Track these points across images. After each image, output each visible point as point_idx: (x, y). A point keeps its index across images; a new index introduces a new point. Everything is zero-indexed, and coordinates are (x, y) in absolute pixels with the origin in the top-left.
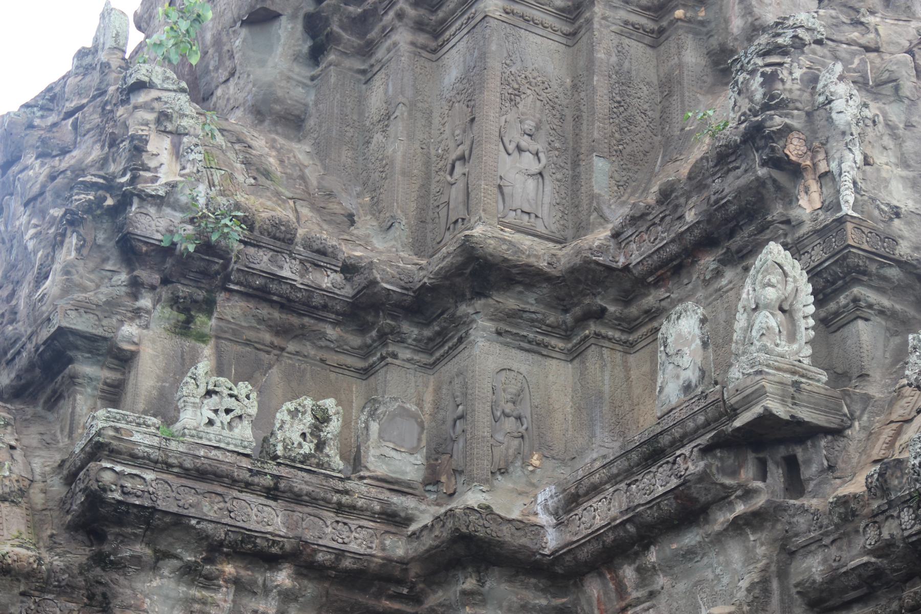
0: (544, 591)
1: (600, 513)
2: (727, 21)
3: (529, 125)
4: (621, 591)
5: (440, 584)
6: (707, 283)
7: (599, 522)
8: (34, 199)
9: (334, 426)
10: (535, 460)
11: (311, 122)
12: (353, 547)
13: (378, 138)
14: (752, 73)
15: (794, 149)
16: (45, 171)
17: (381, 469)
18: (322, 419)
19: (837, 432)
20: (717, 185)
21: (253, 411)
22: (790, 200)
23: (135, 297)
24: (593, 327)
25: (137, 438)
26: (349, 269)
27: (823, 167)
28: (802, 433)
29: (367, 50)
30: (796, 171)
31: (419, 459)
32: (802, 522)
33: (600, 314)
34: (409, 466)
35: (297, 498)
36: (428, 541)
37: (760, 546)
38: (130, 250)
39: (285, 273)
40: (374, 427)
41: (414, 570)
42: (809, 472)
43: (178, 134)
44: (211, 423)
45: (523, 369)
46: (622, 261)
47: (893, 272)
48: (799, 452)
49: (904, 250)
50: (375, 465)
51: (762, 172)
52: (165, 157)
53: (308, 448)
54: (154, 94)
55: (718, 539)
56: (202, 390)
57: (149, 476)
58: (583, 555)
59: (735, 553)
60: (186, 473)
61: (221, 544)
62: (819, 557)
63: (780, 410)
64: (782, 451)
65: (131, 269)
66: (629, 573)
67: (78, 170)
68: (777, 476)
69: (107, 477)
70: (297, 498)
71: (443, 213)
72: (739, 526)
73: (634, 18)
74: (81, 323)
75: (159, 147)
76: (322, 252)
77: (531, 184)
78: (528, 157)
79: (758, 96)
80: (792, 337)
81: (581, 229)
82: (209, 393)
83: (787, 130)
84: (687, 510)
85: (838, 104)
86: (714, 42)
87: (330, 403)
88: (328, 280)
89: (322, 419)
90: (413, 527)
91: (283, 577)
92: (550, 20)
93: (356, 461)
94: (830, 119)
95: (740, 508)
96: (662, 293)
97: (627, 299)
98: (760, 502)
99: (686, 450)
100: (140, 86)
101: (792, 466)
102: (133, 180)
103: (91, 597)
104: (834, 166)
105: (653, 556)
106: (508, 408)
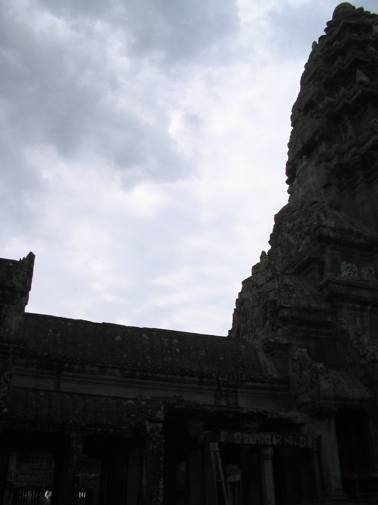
8: (290, 231)
16: (291, 225)
44: (350, 274)
52: (323, 217)
56: (346, 267)
57: (341, 287)
67: (301, 223)
82: (348, 268)
87: (371, 268)
88: (361, 241)
91: (369, 308)
100: (315, 202)
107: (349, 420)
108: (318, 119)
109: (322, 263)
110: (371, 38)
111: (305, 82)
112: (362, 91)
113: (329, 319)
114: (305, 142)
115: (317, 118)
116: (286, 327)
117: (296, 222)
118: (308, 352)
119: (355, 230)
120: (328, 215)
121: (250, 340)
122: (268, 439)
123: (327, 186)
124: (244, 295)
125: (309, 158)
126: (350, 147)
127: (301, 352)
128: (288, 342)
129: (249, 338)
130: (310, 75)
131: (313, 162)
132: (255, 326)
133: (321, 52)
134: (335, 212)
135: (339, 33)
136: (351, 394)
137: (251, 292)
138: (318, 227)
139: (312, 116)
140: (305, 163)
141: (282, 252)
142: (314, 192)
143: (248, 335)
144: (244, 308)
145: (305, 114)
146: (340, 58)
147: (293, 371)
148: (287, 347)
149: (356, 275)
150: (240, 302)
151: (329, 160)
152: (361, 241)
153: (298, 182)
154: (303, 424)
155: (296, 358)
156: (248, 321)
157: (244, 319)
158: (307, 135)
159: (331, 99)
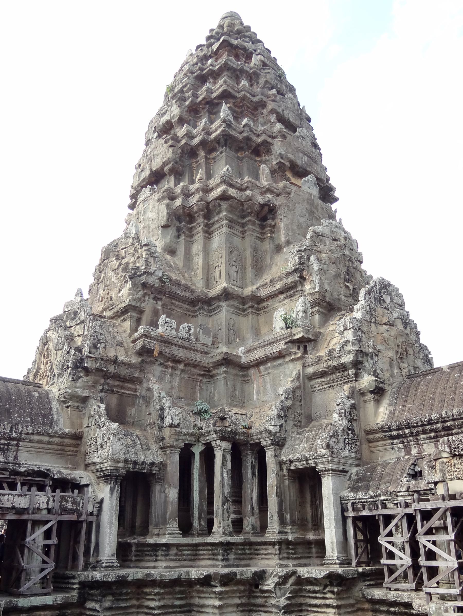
0: (240, 371)
1: (258, 355)
2: (280, 239)
3: (234, 259)
4: (260, 372)
5: (218, 369)
6: (280, 302)
7: (257, 357)
9: (192, 331)
10: (238, 340)
11: (178, 253)
12: (198, 359)
13: (195, 258)
14: (296, 255)
15: (305, 274)
16: (118, 263)
17: (203, 342)
18: (190, 329)
19: (315, 340)
20: (285, 279)
21: (175, 327)
22: (302, 285)
23: (144, 297)
24: (250, 310)
25: (152, 333)
26: (192, 292)
27: (311, 279)
28: (309, 341)
29: (192, 236)
30: (305, 279)
31: (211, 339)
32: (309, 360)
33: (252, 307)
34: (209, 341)
35: (185, 348)
36: (215, 359)
37: (298, 366)
38: (144, 285)
39: (179, 292)
40: (201, 331)
41: (211, 365)
42: (309, 349)
43: (155, 257)
44: (167, 330)
45: (235, 318)
46: (259, 295)
47: (325, 304)
48: (307, 345)
49: (327, 299)
50: (202, 340)
51: (297, 279)
52: (152, 263)
53: (187, 336)
54: (149, 247)
55: (287, 362)
57: (155, 342)
58: (251, 364)
59: (291, 365)
60: (162, 342)
61: (169, 358)
62: (312, 368)
63: (306, 336)
64: (303, 344)
65: (143, 291)
66: (262, 368)
67: (127, 264)
68: (302, 349)
69: (146, 342)
70: (185, 348)
71: (213, 279)
72: (292, 360)
73: (258, 235)
74: (133, 303)
75: (151, 260)
76: (187, 288)
77: (235, 274)
78: (234, 267)
79: (297, 261)
80: (306, 318)
81: (246, 286)
82: (166, 322)
83: (304, 269)
84: (280, 355)
85: (315, 265)
86: (277, 243)
88: (188, 294)
89: (190, 329)
90: (209, 355)
91: (181, 366)
92: (238, 234)
93: (197, 340)
94: (313, 268)
95: (293, 357)
96: (268, 303)
97: (258, 304)
98: (299, 355)
99: (281, 342)
101: (305, 348)
102: (145, 268)
103: (141, 370)
104: (314, 279)
105: (269, 365)
106: (231, 328)
107: (135, 484)
108: (172, 148)
109: (141, 312)
110: (248, 69)
111: (170, 95)
112: (223, 131)
113: (136, 375)
114: (153, 170)
115: (171, 146)
116: (88, 378)
117: (124, 261)
118: (107, 409)
119: (183, 282)
120: (158, 262)
121: (48, 386)
122: (43, 502)
123: (165, 227)
124: (49, 334)
125: (153, 191)
126: (197, 190)
127: (99, 407)
128: (87, 395)
129: (47, 384)
130: (176, 90)
131: (157, 196)
132: (55, 371)
133: (193, 65)
134: (169, 257)
135: (218, 49)
136: (143, 457)
137: (58, 332)
138: (144, 273)
139: (166, 142)
140: (148, 194)
141: (104, 290)
142: (151, 229)
143: (46, 379)
144: (47, 349)
145: (159, 136)
146: (211, 80)
147: (88, 427)
148: (85, 400)
149: (174, 332)
150: (45, 341)
151: (173, 198)
152: (187, 295)
153: (138, 213)
154: (87, 486)
155: (92, 413)
156: (49, 364)
157: (45, 361)
158: (156, 164)
159: (190, 128)
